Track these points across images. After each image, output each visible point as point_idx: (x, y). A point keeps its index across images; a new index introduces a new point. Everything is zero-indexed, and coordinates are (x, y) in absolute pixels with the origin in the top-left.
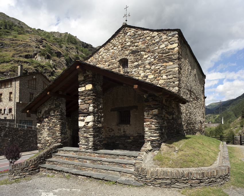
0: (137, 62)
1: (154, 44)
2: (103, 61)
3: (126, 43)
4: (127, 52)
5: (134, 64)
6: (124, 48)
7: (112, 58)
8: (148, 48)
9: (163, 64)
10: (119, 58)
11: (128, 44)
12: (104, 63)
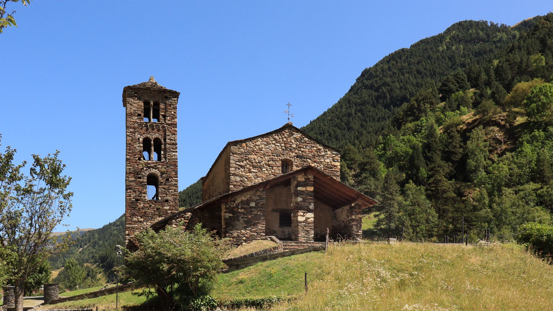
1: (320, 156)
3: (291, 144)
6: (288, 148)
7: (273, 154)
10: (283, 157)
11: (294, 146)
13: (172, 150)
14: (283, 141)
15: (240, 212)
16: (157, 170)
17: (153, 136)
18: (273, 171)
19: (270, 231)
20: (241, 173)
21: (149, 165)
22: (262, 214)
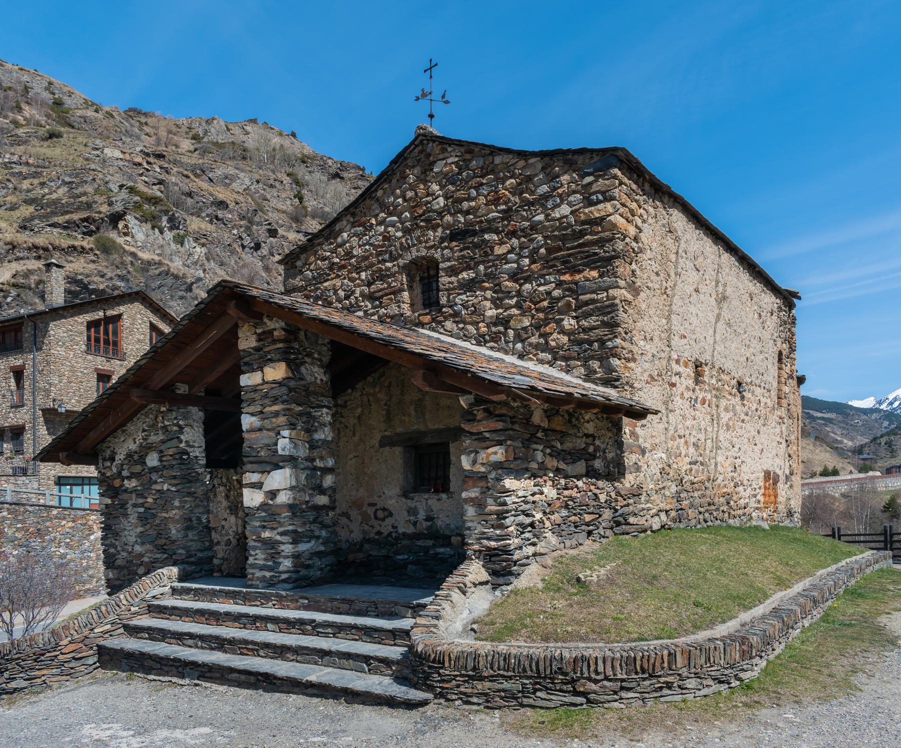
0: (468, 268)
5: (460, 277)
10: (408, 257)
19: (377, 510)
22: (173, 489)
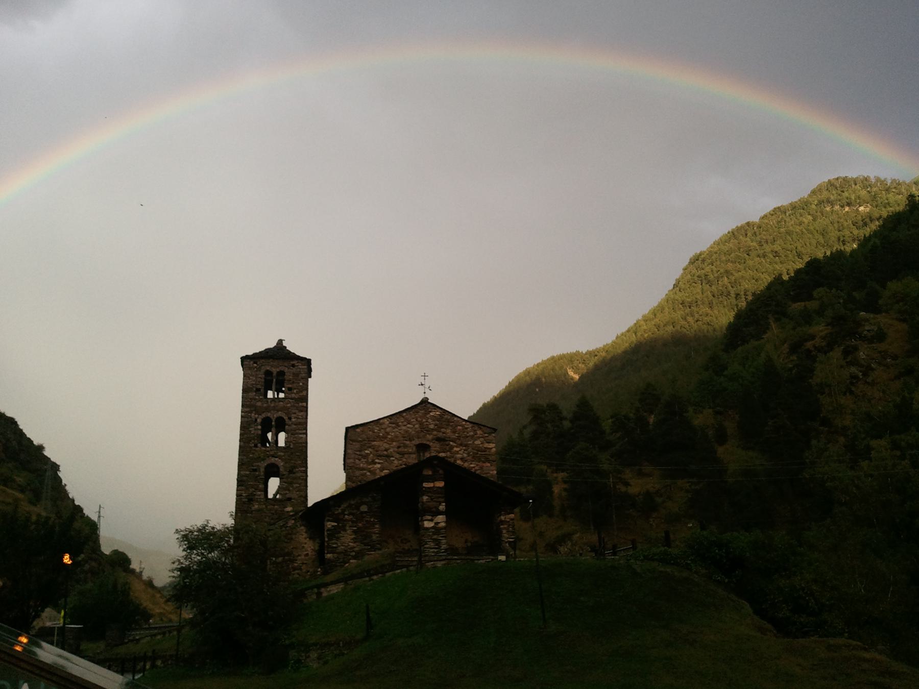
1: (467, 437)
2: (388, 439)
3: (427, 425)
4: (430, 437)
6: (424, 429)
7: (405, 439)
8: (459, 439)
9: (479, 464)
10: (417, 442)
11: (432, 427)
12: (390, 443)
13: (297, 431)
14: (417, 420)
15: (346, 520)
16: (276, 459)
17: (274, 415)
18: (404, 460)
20: (362, 465)
21: (268, 453)
